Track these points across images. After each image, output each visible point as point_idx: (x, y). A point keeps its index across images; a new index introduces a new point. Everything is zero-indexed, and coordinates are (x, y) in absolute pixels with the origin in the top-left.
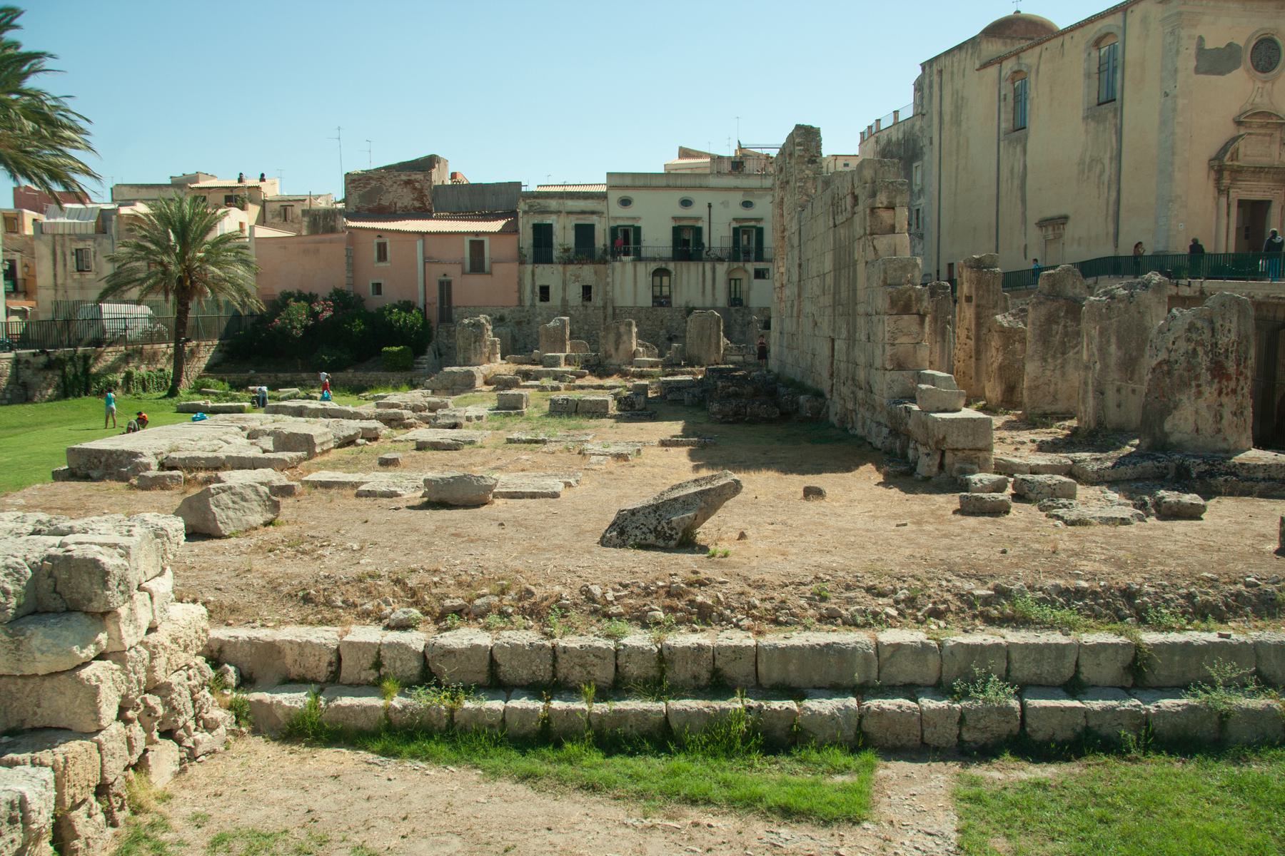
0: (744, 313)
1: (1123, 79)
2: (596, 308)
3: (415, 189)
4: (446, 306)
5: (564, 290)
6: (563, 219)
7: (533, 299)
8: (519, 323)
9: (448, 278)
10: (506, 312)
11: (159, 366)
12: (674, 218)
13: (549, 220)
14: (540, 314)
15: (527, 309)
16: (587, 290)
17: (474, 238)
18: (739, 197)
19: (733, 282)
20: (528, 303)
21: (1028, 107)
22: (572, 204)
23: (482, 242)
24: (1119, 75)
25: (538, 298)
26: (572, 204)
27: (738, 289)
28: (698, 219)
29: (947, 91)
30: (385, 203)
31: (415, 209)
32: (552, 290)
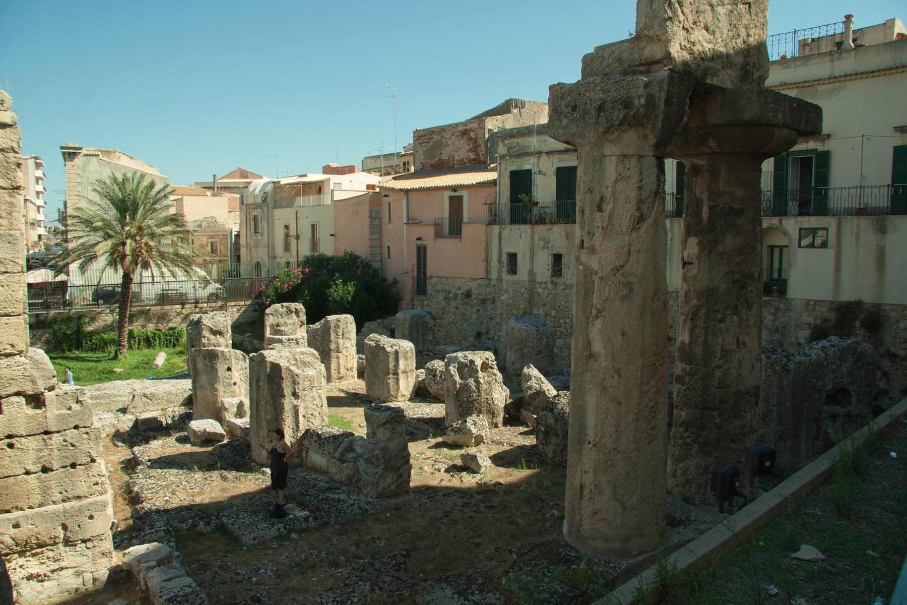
0: (778, 309)
2: (567, 287)
3: (470, 139)
4: (422, 276)
5: (532, 259)
7: (500, 271)
8: (484, 301)
9: (425, 243)
10: (473, 285)
11: (171, 325)
13: (528, 164)
14: (506, 291)
15: (493, 283)
19: (776, 252)
20: (494, 275)
23: (460, 198)
25: (504, 270)
27: (776, 265)
30: (445, 157)
31: (470, 161)
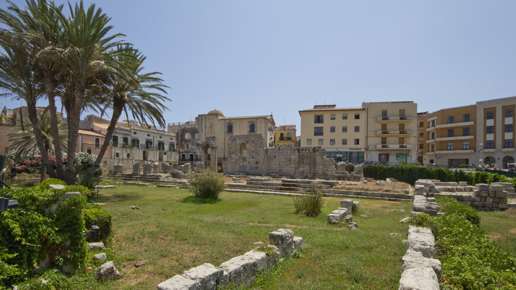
1: (257, 129)
5: (123, 154)
6: (120, 135)
7: (114, 157)
9: (90, 149)
12: (146, 139)
16: (128, 155)
17: (96, 137)
18: (159, 136)
21: (233, 129)
22: (122, 132)
24: (255, 128)
26: (122, 132)
28: (151, 140)
29: (208, 122)
32: (119, 154)
